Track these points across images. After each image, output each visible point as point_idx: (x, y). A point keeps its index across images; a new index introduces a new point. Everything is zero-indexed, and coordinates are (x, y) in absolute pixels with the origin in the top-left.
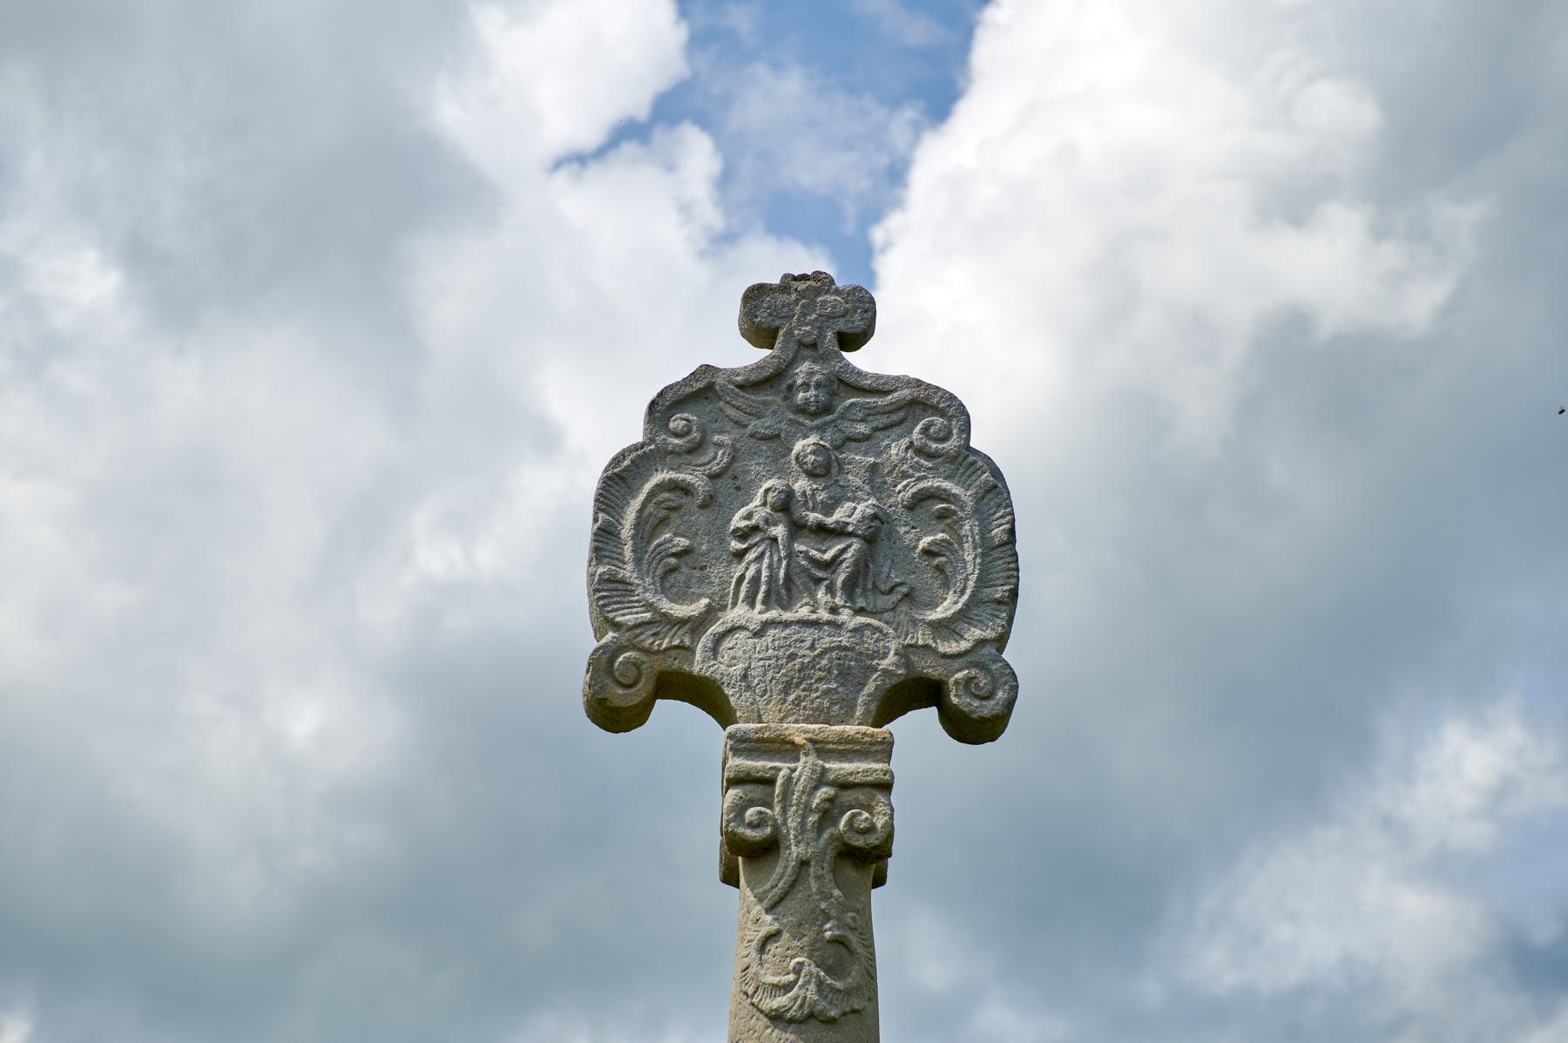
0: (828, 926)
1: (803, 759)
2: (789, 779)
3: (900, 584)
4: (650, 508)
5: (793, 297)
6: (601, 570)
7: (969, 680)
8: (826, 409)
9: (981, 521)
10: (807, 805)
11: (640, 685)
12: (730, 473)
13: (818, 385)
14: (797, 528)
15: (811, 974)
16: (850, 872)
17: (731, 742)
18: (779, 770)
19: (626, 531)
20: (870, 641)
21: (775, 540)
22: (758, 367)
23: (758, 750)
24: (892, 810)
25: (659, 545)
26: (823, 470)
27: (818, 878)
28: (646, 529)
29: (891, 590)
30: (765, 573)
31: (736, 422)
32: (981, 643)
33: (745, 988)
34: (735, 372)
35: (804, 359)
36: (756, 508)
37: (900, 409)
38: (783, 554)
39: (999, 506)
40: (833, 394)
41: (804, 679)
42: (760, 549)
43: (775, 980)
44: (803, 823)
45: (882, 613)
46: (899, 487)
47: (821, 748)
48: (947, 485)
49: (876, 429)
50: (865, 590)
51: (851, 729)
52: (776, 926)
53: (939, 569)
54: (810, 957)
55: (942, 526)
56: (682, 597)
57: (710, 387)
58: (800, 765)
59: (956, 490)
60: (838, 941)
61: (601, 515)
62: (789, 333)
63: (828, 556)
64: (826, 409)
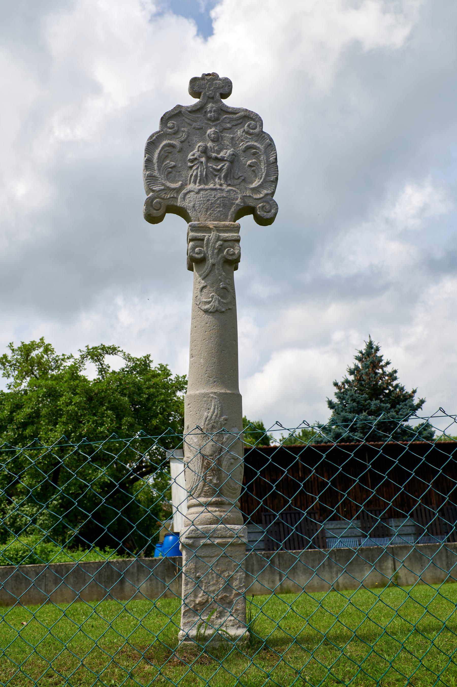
0: (221, 284)
1: (212, 233)
2: (208, 239)
3: (241, 176)
4: (162, 153)
5: (206, 81)
6: (148, 173)
7: (263, 207)
8: (217, 119)
9: (266, 155)
10: (214, 247)
11: (161, 209)
12: (187, 141)
13: (214, 111)
14: (209, 158)
15: (216, 298)
16: (227, 267)
17: (190, 228)
18: (205, 236)
19: (155, 160)
20: (232, 194)
21: (202, 162)
22: (195, 105)
23: (199, 230)
24: (240, 248)
25: (166, 165)
26: (217, 139)
27: (218, 269)
28: (161, 159)
29: (239, 178)
30: (199, 173)
31: (189, 124)
32: (267, 195)
33: (196, 303)
34: (188, 107)
35: (210, 102)
36: (195, 152)
37: (240, 119)
38: (205, 167)
39: (272, 150)
40: (219, 114)
41: (212, 207)
42: (197, 166)
43: (206, 300)
44: (213, 252)
45: (236, 185)
46: (241, 145)
47: (218, 229)
48: (256, 144)
49: (233, 126)
50: (230, 178)
51: (227, 223)
52: (205, 284)
53: (253, 171)
54: (216, 293)
55: (254, 157)
56: (173, 181)
57: (180, 112)
58: (212, 234)
59: (259, 145)
60: (224, 288)
61: (147, 155)
62: (205, 94)
63: (219, 167)
64: (217, 119)
